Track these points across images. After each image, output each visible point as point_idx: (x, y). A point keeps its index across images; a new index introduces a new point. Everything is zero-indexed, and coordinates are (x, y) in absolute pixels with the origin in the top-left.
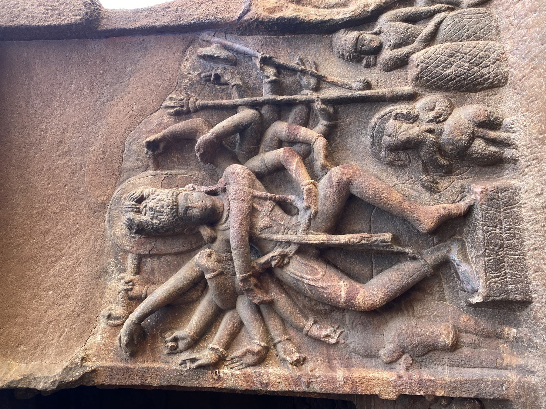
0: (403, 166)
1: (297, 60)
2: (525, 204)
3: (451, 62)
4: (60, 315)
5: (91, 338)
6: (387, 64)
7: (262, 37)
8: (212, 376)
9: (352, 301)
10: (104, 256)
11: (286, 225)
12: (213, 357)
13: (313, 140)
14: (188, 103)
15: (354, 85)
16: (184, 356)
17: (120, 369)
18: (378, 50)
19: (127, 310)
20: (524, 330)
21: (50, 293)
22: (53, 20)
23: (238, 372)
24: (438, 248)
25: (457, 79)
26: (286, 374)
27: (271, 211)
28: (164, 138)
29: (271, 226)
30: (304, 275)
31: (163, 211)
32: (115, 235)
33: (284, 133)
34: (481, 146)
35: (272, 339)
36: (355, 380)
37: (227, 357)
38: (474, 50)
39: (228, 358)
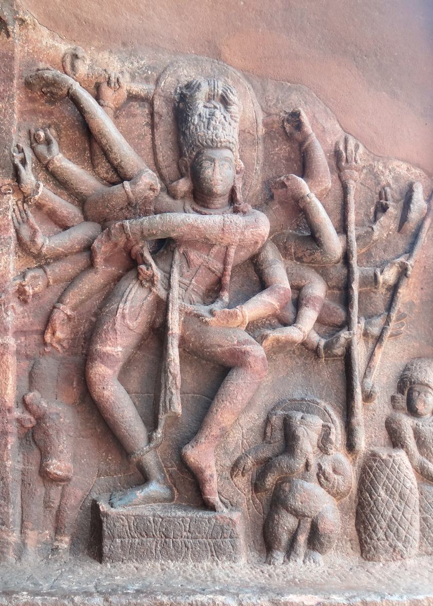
2: (217, 565)
6: (394, 422)
8: (5, 185)
9: (99, 359)
11: (191, 287)
12: (29, 187)
13: (299, 326)
14: (350, 168)
15: (369, 381)
16: (29, 154)
18: (413, 411)
23: (10, 217)
24: (163, 472)
25: (372, 503)
26: (10, 275)
27: (209, 269)
28: (306, 137)
29: (189, 267)
30: (128, 303)
32: (179, 67)
33: (310, 291)
34: (287, 525)
36: (5, 357)
37: (28, 204)
38: (408, 523)
39: (25, 205)
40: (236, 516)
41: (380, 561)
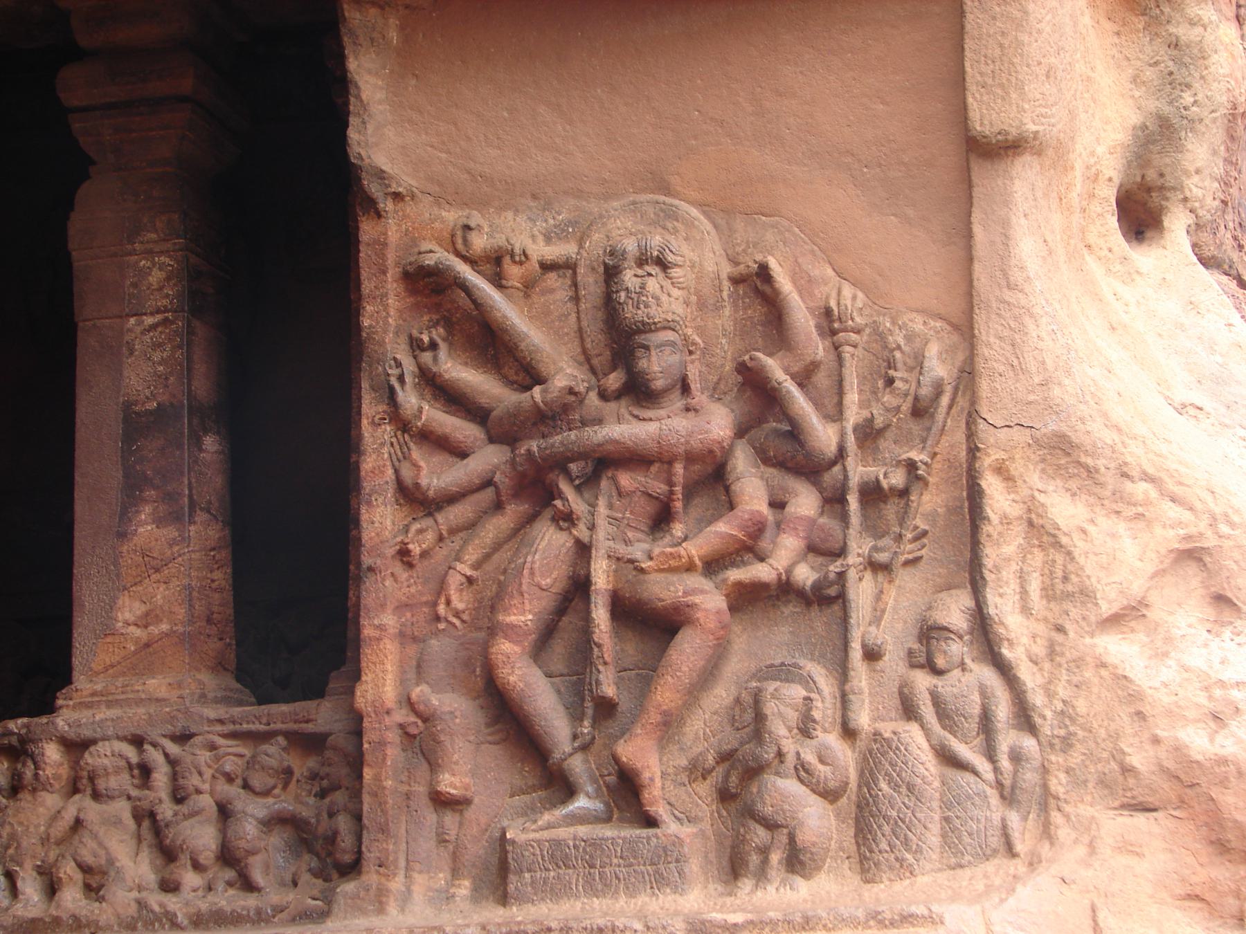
0: (733, 720)
1: (923, 526)
3: (900, 787)
4: (469, 139)
5: (431, 199)
7: (964, 460)
10: (572, 202)
14: (845, 330)
16: (409, 366)
17: (383, 257)
19: (480, 257)
20: (466, 906)
21: (506, 114)
22: (973, 77)
23: (386, 456)
27: (650, 495)
28: (777, 292)
31: (638, 308)
32: (609, 217)
35: (439, 508)
40: (686, 831)
41: (882, 882)
